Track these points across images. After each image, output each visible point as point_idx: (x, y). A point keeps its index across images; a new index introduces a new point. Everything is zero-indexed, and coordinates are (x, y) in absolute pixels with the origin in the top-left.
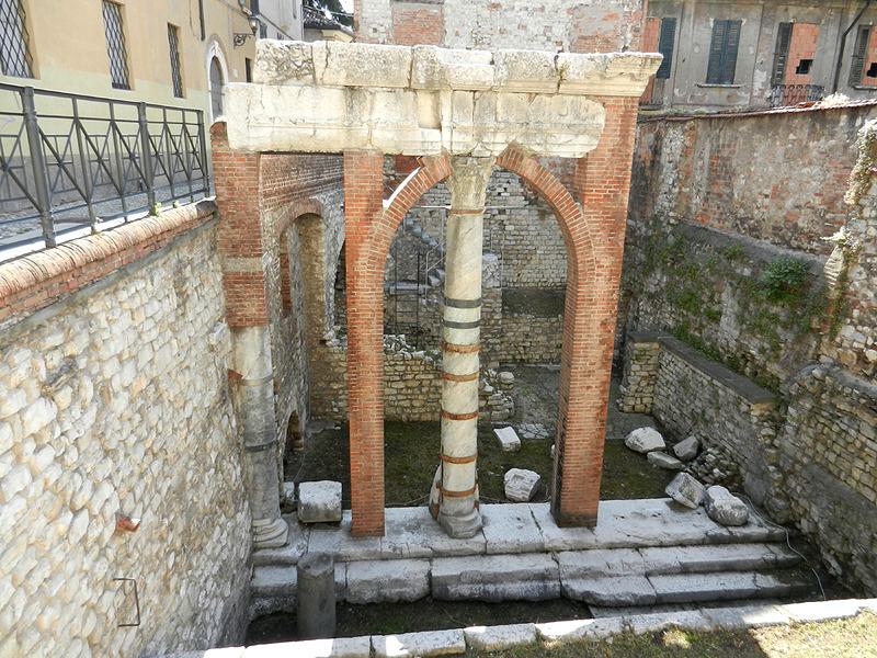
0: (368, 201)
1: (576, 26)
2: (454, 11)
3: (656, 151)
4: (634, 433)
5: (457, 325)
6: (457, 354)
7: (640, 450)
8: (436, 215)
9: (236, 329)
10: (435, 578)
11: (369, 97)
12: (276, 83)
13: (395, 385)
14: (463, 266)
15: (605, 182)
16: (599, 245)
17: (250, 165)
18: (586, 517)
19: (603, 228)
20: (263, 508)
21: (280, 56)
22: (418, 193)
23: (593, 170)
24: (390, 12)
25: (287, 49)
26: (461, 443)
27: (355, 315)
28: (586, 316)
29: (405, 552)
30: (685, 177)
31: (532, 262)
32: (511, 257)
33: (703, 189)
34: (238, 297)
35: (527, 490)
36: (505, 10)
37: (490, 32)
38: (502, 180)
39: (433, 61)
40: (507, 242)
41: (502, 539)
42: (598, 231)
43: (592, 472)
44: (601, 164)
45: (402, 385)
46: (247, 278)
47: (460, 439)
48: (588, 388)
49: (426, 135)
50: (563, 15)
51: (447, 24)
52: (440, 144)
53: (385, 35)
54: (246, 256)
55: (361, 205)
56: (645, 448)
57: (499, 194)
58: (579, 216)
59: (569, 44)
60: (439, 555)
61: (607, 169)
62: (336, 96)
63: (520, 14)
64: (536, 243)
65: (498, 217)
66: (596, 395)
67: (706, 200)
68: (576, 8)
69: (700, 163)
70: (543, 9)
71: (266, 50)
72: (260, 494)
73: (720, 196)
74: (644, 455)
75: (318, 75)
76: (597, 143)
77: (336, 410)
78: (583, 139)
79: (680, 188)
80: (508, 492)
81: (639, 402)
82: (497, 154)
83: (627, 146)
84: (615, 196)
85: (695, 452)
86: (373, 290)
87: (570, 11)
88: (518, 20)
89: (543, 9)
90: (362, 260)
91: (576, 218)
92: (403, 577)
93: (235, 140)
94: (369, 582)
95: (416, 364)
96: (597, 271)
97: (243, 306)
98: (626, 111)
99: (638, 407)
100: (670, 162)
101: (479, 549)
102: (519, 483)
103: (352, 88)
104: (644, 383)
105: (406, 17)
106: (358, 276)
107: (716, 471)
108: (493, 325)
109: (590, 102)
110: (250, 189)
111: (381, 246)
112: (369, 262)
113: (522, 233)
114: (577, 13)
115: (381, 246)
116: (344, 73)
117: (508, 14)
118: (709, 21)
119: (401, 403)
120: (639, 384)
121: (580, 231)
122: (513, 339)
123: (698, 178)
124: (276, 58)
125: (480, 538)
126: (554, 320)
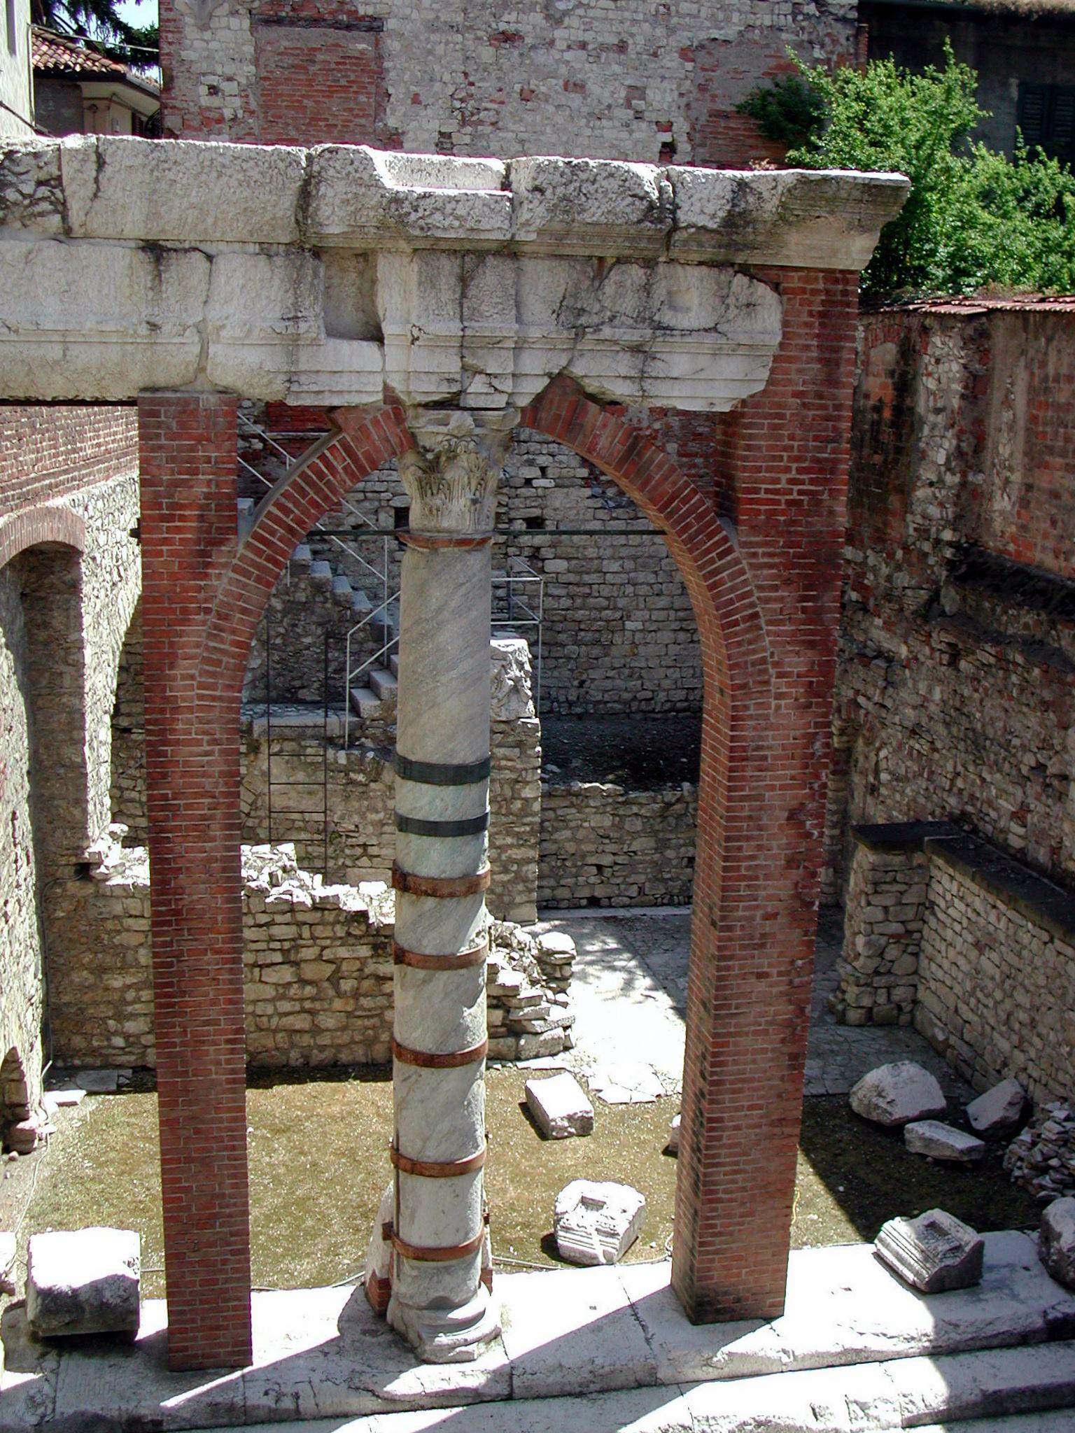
1: (702, 88)
2: (407, 47)
3: (904, 384)
4: (872, 1077)
7: (886, 1119)
13: (271, 976)
16: (780, 622)
19: (787, 582)
23: (758, 434)
24: (249, 49)
30: (973, 449)
31: (614, 651)
32: (562, 637)
33: (1016, 477)
35: (613, 1235)
36: (533, 47)
37: (497, 96)
38: (534, 447)
39: (359, 182)
40: (551, 603)
42: (775, 588)
45: (287, 974)
48: (760, 976)
50: (671, 61)
51: (392, 75)
53: (237, 102)
56: (898, 1113)
57: (528, 482)
58: (729, 551)
59: (686, 127)
62: (123, 263)
63: (568, 56)
65: (525, 540)
67: (1024, 503)
68: (702, 47)
69: (1007, 416)
70: (622, 47)
73: (1055, 495)
74: (896, 1130)
77: (119, 1041)
78: (732, 367)
79: (964, 475)
81: (882, 999)
84: (818, 503)
85: (1014, 1115)
86: (215, 742)
87: (686, 54)
88: (563, 70)
89: (622, 47)
90: (185, 667)
91: (721, 556)
95: (322, 923)
100: (937, 411)
102: (591, 1219)
104: (892, 952)
105: (289, 61)
106: (176, 710)
113: (586, 578)
114: (702, 57)
115: (234, 632)
117: (541, 57)
118: (1005, 85)
121: (732, 589)
122: (571, 847)
123: (1005, 451)
126: (670, 796)
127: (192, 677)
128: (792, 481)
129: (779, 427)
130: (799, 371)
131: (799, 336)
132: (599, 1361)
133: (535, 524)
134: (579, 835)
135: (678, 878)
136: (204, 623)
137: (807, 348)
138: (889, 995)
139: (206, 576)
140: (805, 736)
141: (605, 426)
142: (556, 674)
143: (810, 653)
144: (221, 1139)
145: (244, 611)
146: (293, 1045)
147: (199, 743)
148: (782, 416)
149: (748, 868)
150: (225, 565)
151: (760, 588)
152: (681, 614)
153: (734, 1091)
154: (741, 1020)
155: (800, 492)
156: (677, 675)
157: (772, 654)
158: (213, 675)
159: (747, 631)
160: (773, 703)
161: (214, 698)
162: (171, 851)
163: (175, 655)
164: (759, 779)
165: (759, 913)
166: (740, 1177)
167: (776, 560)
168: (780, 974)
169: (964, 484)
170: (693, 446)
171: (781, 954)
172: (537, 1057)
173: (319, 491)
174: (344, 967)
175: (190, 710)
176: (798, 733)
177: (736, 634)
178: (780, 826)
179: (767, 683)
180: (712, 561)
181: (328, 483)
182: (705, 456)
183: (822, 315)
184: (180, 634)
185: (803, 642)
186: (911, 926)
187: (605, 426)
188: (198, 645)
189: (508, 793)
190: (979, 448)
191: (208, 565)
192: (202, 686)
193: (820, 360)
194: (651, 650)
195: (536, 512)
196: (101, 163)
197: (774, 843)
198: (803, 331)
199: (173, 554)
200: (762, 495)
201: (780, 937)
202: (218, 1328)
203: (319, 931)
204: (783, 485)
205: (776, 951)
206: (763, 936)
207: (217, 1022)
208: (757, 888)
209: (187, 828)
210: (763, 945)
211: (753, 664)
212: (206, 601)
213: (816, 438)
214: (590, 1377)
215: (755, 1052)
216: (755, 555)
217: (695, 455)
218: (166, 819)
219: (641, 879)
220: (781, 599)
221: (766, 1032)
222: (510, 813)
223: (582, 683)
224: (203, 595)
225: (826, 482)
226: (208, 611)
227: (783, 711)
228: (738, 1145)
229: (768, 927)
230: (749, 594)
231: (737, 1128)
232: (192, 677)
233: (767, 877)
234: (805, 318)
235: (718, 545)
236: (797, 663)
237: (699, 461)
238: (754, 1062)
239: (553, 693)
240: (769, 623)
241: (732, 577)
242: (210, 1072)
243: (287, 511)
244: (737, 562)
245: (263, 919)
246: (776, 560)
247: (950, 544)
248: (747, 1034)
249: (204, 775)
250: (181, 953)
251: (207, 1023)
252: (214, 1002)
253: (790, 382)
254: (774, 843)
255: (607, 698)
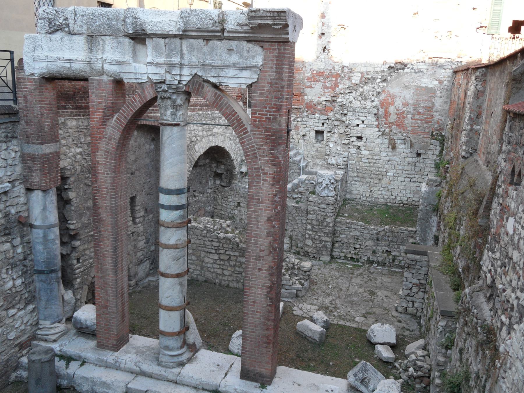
0: (103, 112)
5: (163, 207)
6: (162, 229)
7: (372, 341)
8: (306, 138)
9: (29, 190)
10: (130, 388)
11: (101, 42)
12: (50, 33)
13: (212, 256)
14: (165, 163)
15: (266, 108)
16: (264, 156)
17: (36, 85)
18: (261, 376)
19: (266, 143)
20: (46, 313)
21: (50, 17)
22: (134, 109)
25: (55, 13)
26: (166, 295)
27: (96, 190)
28: (255, 211)
29: (122, 366)
31: (383, 182)
34: (30, 169)
38: (360, 114)
39: (136, 18)
40: (361, 164)
41: (191, 375)
42: (262, 145)
43: (265, 340)
44: (261, 93)
45: (216, 257)
46: (34, 158)
47: (170, 292)
48: (260, 269)
49: (137, 67)
52: (146, 75)
54: (33, 143)
55: (99, 115)
57: (358, 125)
58: (247, 132)
60: (143, 374)
61: (267, 97)
62: (80, 41)
64: (386, 166)
66: (265, 277)
71: (42, 12)
72: (43, 303)
74: (373, 345)
75: (71, 28)
76: (257, 77)
78: (246, 74)
79: (472, 126)
80: (230, 347)
81: (410, 305)
82: (184, 83)
83: (282, 80)
92: (109, 382)
93: (28, 69)
94: (87, 379)
95: (226, 243)
96: (262, 176)
97: (32, 176)
98: (279, 53)
99: (410, 310)
101: (171, 377)
103: (92, 36)
104: (415, 290)
106: (98, 164)
107: (411, 369)
108: (326, 226)
109: (250, 45)
110: (36, 101)
111: (112, 144)
112: (105, 154)
113: (375, 157)
115: (112, 144)
116: (85, 27)
119: (216, 270)
120: (411, 289)
121: (248, 145)
124: (48, 18)
125: (176, 370)
127: (102, 155)
128: (266, 111)
129: (263, 93)
130: (269, 75)
131: (269, 64)
132: (203, 379)
133: (360, 138)
134: (349, 237)
135: (381, 256)
136: (105, 141)
137: (272, 68)
138: (413, 304)
139: (105, 128)
140: (273, 194)
141: (209, 91)
142: (363, 187)
143: (273, 167)
144: (109, 285)
145: (115, 139)
146: (217, 278)
147: (104, 174)
148: (263, 90)
149: (254, 234)
150: (109, 126)
151: (257, 145)
152: (407, 172)
153: (251, 305)
154: (253, 282)
155: (270, 115)
156: (404, 192)
157: (261, 166)
158: (107, 155)
159: (252, 158)
160: (262, 182)
161: (107, 162)
162: (97, 202)
163: (98, 149)
164: (257, 206)
165: (258, 249)
166: (254, 334)
167: (262, 136)
168: (265, 270)
169: (471, 130)
170: (417, 117)
171: (266, 264)
172: (286, 297)
173: (132, 107)
174: (232, 258)
175: (101, 164)
176: (270, 193)
177: (249, 159)
178: (265, 222)
179: (260, 175)
180: (241, 135)
181: (135, 105)
182: (422, 120)
183: (277, 57)
184: (99, 143)
185: (271, 164)
186: (422, 282)
187: (209, 91)
188: (104, 147)
189: (322, 219)
190: (479, 116)
191: (106, 125)
192: (105, 158)
193: (276, 72)
194: (396, 183)
195: (360, 135)
196: (76, 15)
197: (263, 227)
198: (270, 62)
199: (97, 121)
200: (257, 115)
201: (265, 258)
202: (108, 339)
203: (225, 246)
204: (264, 112)
205: (264, 262)
206: (260, 256)
207: (109, 252)
208: (257, 241)
209: (101, 197)
210: (260, 260)
211: (255, 169)
212: (105, 135)
213: (275, 98)
214: (199, 383)
215: (258, 294)
216: (255, 134)
217: (418, 120)
218: (96, 193)
219: (369, 254)
220: (264, 149)
221: (261, 288)
222: (322, 225)
223: (371, 191)
224: (104, 133)
225: (278, 112)
226: (106, 138)
227: (265, 185)
228: (253, 323)
229: (261, 254)
230: (253, 146)
231: (253, 317)
232: (102, 155)
233: (260, 238)
234: (271, 58)
235: (243, 130)
236: (270, 170)
237: (419, 122)
238: (258, 297)
239: (361, 193)
240: (260, 156)
241: (248, 141)
242: (106, 265)
243: (125, 112)
244: (249, 136)
245: (211, 239)
246: (262, 136)
247: (465, 150)
248: (255, 288)
249: (105, 183)
250: (100, 231)
251: (106, 251)
252: (108, 246)
253: (266, 79)
254: (263, 227)
255: (379, 197)
